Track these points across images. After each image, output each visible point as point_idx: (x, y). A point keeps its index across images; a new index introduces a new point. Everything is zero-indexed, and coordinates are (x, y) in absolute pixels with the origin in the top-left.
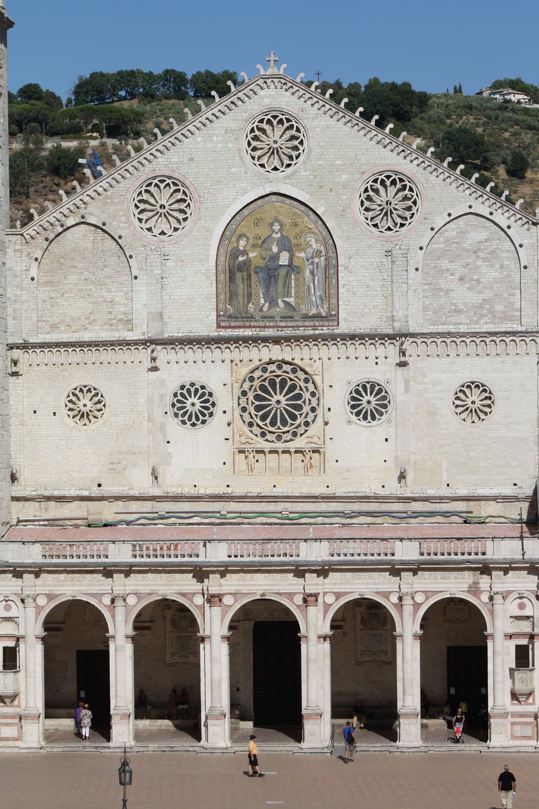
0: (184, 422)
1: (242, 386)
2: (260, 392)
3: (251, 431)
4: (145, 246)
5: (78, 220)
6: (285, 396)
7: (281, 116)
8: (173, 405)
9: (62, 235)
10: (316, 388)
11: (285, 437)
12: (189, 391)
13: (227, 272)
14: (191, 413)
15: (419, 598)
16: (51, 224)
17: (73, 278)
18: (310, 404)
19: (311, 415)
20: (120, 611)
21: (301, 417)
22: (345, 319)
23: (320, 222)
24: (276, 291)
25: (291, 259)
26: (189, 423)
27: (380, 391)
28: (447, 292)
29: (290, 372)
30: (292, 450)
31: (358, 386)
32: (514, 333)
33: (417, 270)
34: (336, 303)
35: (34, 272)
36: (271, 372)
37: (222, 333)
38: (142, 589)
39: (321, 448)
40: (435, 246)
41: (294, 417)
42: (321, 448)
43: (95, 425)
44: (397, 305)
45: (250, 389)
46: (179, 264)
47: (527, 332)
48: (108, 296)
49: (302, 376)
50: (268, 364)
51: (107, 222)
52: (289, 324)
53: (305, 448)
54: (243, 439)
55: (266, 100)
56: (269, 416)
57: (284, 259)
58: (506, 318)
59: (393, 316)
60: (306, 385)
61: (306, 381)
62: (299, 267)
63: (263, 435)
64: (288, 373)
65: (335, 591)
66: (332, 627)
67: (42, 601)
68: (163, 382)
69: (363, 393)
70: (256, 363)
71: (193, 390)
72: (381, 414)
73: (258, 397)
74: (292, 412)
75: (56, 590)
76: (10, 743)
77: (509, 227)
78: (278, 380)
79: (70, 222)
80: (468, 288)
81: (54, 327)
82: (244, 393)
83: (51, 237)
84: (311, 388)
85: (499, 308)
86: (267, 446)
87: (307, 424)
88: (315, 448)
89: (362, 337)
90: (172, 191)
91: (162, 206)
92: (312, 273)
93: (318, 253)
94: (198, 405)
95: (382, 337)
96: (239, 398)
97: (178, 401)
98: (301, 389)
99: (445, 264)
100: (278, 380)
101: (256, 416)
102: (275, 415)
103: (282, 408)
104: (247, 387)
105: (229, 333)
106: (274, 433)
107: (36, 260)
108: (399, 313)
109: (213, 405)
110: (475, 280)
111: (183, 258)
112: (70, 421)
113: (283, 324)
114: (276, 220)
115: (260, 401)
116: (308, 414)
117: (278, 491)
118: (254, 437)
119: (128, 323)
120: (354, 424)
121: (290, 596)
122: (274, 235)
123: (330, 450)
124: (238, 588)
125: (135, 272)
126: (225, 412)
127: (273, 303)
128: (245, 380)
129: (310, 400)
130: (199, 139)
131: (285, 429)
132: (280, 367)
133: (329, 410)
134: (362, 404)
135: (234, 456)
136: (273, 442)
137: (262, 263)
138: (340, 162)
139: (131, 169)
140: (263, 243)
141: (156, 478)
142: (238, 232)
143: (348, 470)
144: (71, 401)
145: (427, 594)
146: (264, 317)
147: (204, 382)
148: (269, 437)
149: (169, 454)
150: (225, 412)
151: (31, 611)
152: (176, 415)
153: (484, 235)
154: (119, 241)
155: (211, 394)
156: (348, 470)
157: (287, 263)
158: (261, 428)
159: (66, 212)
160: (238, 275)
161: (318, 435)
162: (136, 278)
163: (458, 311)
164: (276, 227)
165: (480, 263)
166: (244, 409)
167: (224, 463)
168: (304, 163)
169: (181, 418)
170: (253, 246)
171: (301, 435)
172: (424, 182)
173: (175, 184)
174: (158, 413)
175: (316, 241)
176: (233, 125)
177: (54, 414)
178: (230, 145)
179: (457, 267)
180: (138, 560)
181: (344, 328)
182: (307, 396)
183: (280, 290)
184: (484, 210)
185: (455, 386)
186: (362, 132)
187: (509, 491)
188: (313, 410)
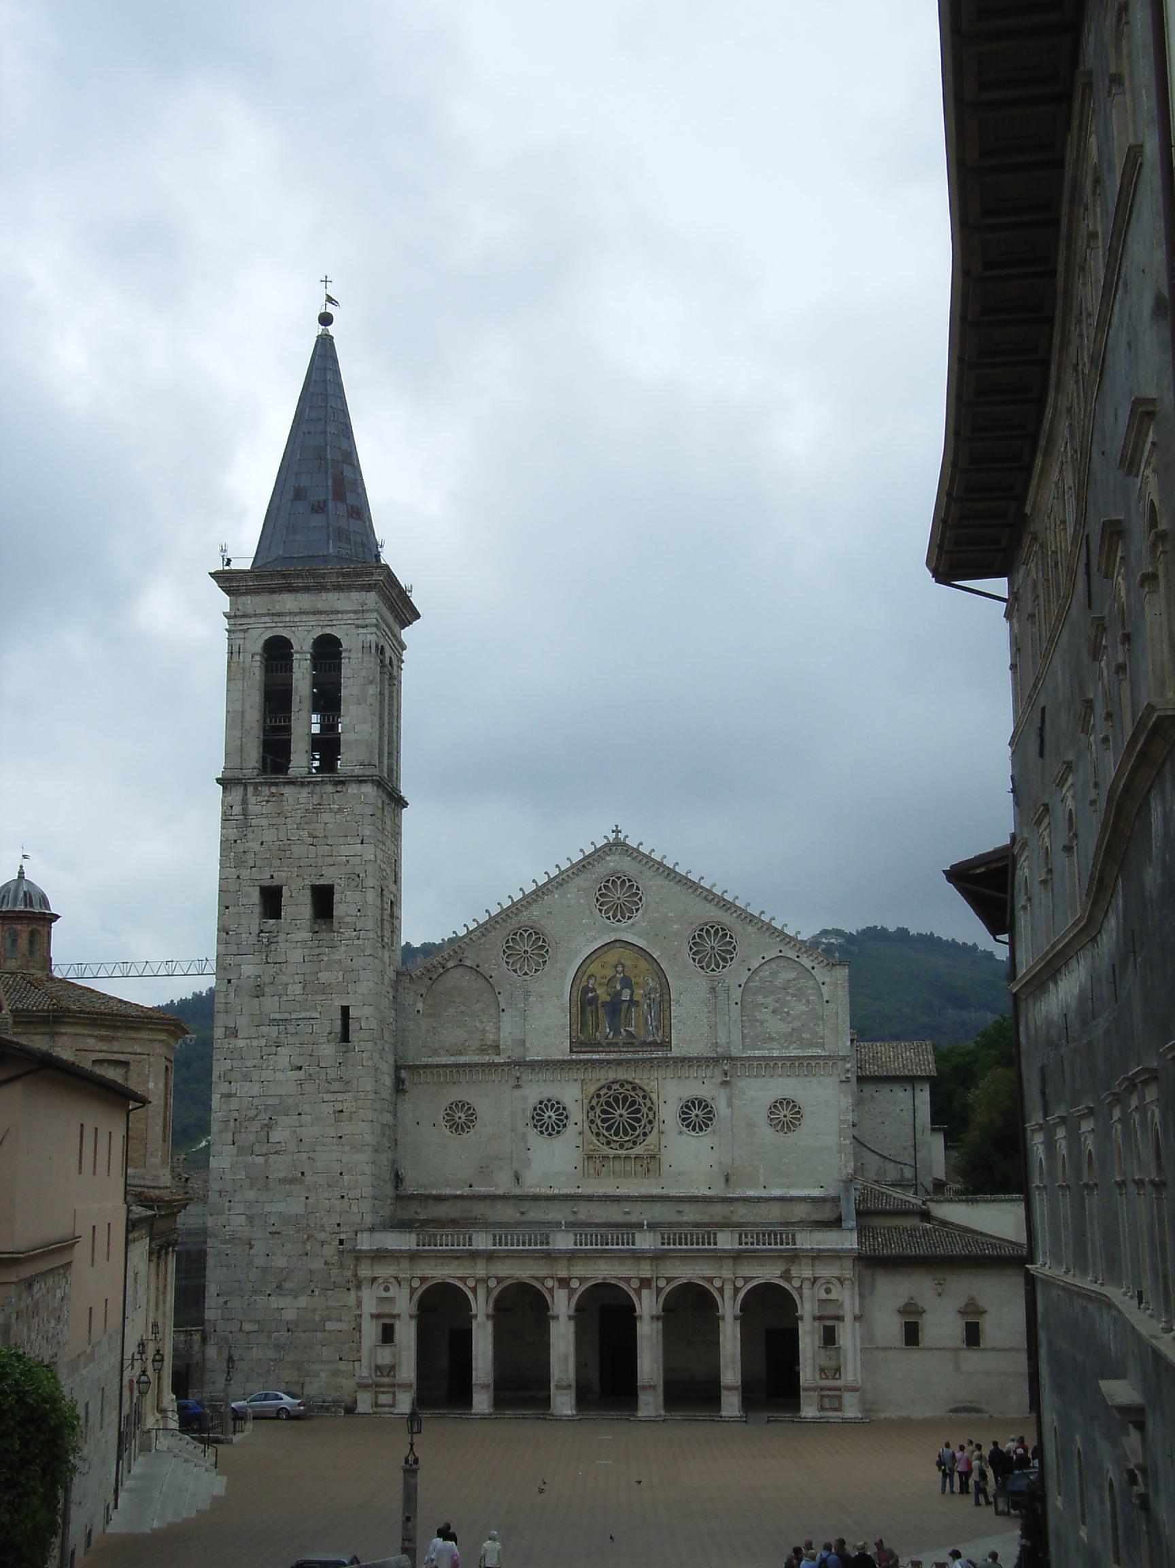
0: (542, 1132)
1: (590, 1103)
2: (605, 1107)
3: (598, 1140)
4: (511, 984)
6: (626, 1110)
7: (623, 878)
8: (533, 1118)
9: (443, 976)
10: (652, 1104)
11: (626, 1145)
12: (546, 1106)
13: (579, 1006)
14: (548, 1125)
15: (740, 1283)
16: (435, 967)
17: (451, 1011)
18: (647, 1117)
19: (649, 1127)
20: (481, 1292)
22: (677, 1045)
23: (655, 964)
24: (620, 1022)
25: (632, 995)
26: (546, 1133)
27: (707, 1106)
28: (762, 1022)
31: (688, 1102)
32: (819, 1057)
33: (737, 1003)
34: (669, 1032)
35: (420, 1006)
36: (615, 1090)
37: (574, 1057)
38: (501, 1274)
40: (751, 984)
41: (634, 1129)
44: (720, 1034)
45: (597, 1105)
46: (539, 999)
47: (830, 1056)
49: (641, 1094)
50: (613, 1083)
51: (481, 964)
52: (630, 1049)
54: (591, 1147)
57: (626, 996)
58: (812, 1044)
59: (716, 1043)
61: (644, 1097)
62: (638, 1002)
63: (608, 1143)
66: (663, 1311)
67: (416, 1283)
68: (524, 1099)
69: (693, 1109)
70: (603, 1082)
71: (549, 1105)
72: (707, 1126)
73: (604, 1112)
75: (429, 1273)
76: (386, 1409)
77: (813, 968)
78: (620, 1097)
79: (450, 964)
80: (780, 1020)
81: (435, 1053)
82: (593, 1108)
83: (434, 977)
84: (649, 1105)
85: (806, 1036)
86: (612, 1153)
87: (645, 1134)
89: (690, 1059)
90: (533, 939)
91: (526, 952)
92: (649, 1006)
93: (654, 990)
94: (554, 1117)
95: (708, 1059)
96: (588, 1112)
97: (537, 1114)
98: (640, 1105)
99: (760, 999)
100: (620, 1097)
101: (603, 1127)
102: (618, 1126)
105: (582, 1056)
106: (617, 1142)
107: (422, 996)
108: (723, 1040)
109: (567, 1117)
110: (786, 1013)
111: (543, 994)
112: (447, 1132)
113: (625, 1049)
114: (620, 963)
116: (645, 1126)
117: (622, 1191)
118: (600, 1145)
119: (496, 1049)
120: (685, 1135)
121: (627, 1280)
122: (618, 975)
123: (666, 1157)
125: (502, 1006)
126: (576, 1124)
127: (617, 1033)
129: (647, 1114)
130: (556, 896)
131: (627, 1139)
132: (622, 1086)
133: (664, 1122)
134: (691, 1118)
137: (608, 999)
139: (500, 921)
140: (608, 982)
141: (518, 1180)
142: (588, 973)
143: (679, 1174)
145: (747, 1280)
146: (609, 1044)
150: (576, 1124)
151: (406, 1291)
152: (535, 1126)
153: (793, 975)
154: (490, 980)
155: (564, 1109)
156: (679, 1174)
157: (628, 998)
158: (607, 1137)
159: (446, 957)
160: (589, 1008)
162: (503, 1010)
163: (771, 1039)
164: (620, 969)
165: (789, 998)
166: (592, 1122)
167: (576, 1168)
168: (643, 915)
169: (539, 1129)
170: (600, 984)
171: (640, 1144)
172: (741, 931)
173: (536, 933)
174: (520, 1124)
175: (653, 979)
176: (584, 885)
177: (434, 1125)
178: (582, 901)
179: (769, 1000)
180: (498, 1247)
181: (676, 1052)
182: (645, 1110)
183: (622, 1021)
184: (792, 954)
185: (769, 1103)
187: (816, 1192)
188: (650, 1122)
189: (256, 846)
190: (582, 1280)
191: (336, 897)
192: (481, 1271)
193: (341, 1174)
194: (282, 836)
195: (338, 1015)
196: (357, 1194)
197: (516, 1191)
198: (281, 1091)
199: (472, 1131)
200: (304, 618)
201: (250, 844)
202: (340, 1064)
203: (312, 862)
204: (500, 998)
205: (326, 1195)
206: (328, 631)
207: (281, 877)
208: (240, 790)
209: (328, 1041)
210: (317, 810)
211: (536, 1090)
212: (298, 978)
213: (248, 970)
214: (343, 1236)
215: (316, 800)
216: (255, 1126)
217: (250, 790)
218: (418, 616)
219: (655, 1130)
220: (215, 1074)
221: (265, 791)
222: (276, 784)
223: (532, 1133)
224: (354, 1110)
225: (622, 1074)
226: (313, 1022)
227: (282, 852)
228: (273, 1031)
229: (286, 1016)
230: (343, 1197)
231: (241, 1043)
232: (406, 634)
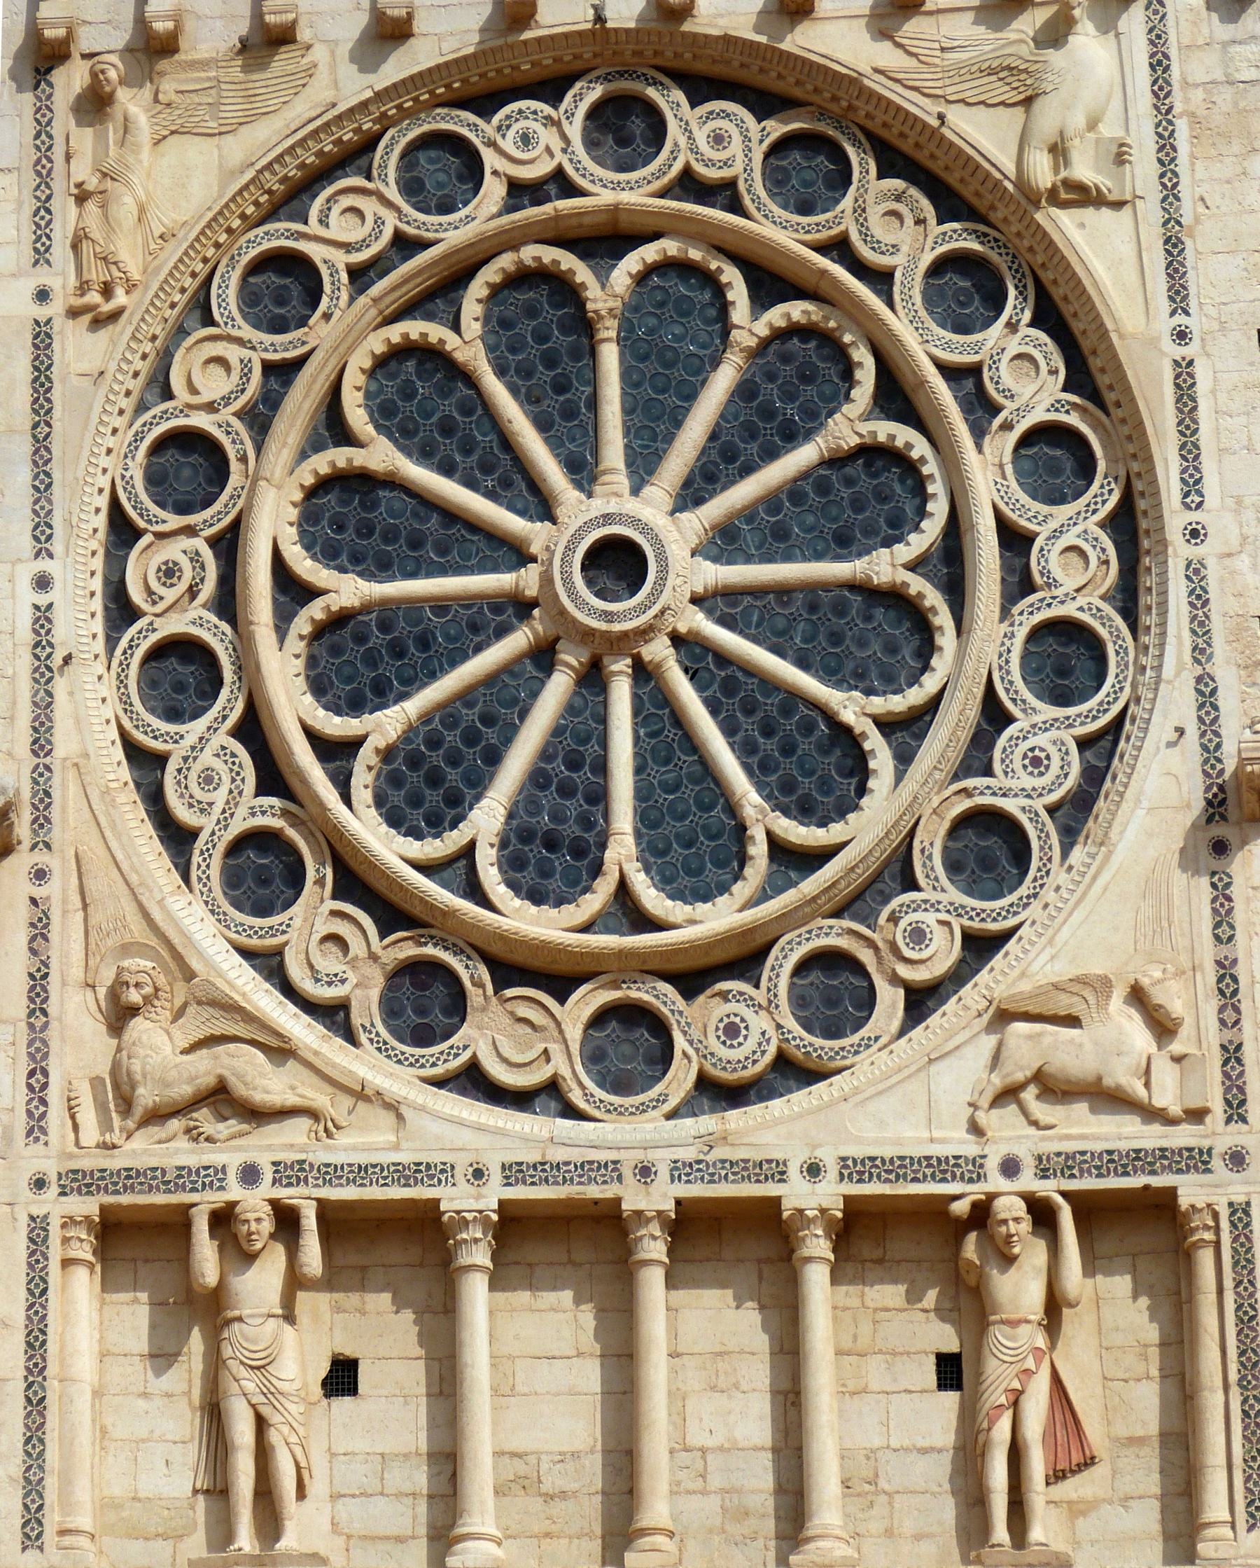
21: (904, 759)
29: (755, 189)
36: (519, 192)
39: (1198, 1160)
42: (1198, 1160)
53: (976, 1169)
56: (494, 758)
60: (959, 349)
64: (736, 207)
74: (793, 698)
88: (1112, 1161)
103: (659, 650)
104: (214, 385)
115: (382, 568)
128: (201, 308)
135: (38, 1290)
161: (1150, 976)
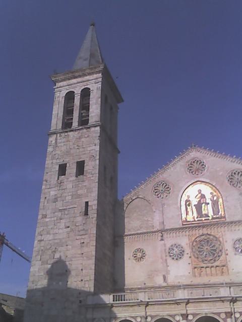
5: (136, 197)
17: (135, 215)
30: (215, 266)
38: (153, 314)
43: (143, 262)
48: (146, 219)
55: (192, 156)
65: (240, 311)
68: (165, 245)
86: (205, 265)
87: (219, 256)
109: (183, 251)
112: (134, 261)
121: (219, 314)
124: (195, 311)
125: (154, 210)
136: (206, 264)
137: (196, 203)
138: (218, 169)
143: (238, 273)
144: (135, 257)
146: (198, 220)
147: (179, 243)
148: (205, 262)
149: (169, 271)
152: (170, 256)
156: (238, 273)
176: (182, 164)
186: (225, 159)
188: (221, 251)
189: (59, 152)
190: (194, 315)
191: (85, 164)
192: (143, 314)
193: (82, 270)
194: (68, 147)
195: (84, 205)
196: (88, 278)
197: (165, 284)
198: (61, 237)
199: (144, 260)
200: (78, 84)
201: (57, 152)
202: (84, 223)
203: (78, 154)
204: (153, 208)
205: (75, 280)
206: (86, 87)
207: (66, 160)
208: (55, 135)
209: (80, 216)
210: (80, 138)
211: (170, 240)
212: (70, 194)
213: (52, 193)
214: (81, 299)
215: (80, 135)
216: (50, 252)
217: (58, 135)
218: (123, 101)
219: (224, 254)
220: (37, 233)
221: (63, 135)
222: (67, 132)
223: (169, 260)
224: (89, 241)
225: (205, 231)
226: (75, 209)
227: (68, 153)
228: (59, 214)
229: (65, 208)
230: (82, 280)
231: (47, 220)
232: (119, 105)
